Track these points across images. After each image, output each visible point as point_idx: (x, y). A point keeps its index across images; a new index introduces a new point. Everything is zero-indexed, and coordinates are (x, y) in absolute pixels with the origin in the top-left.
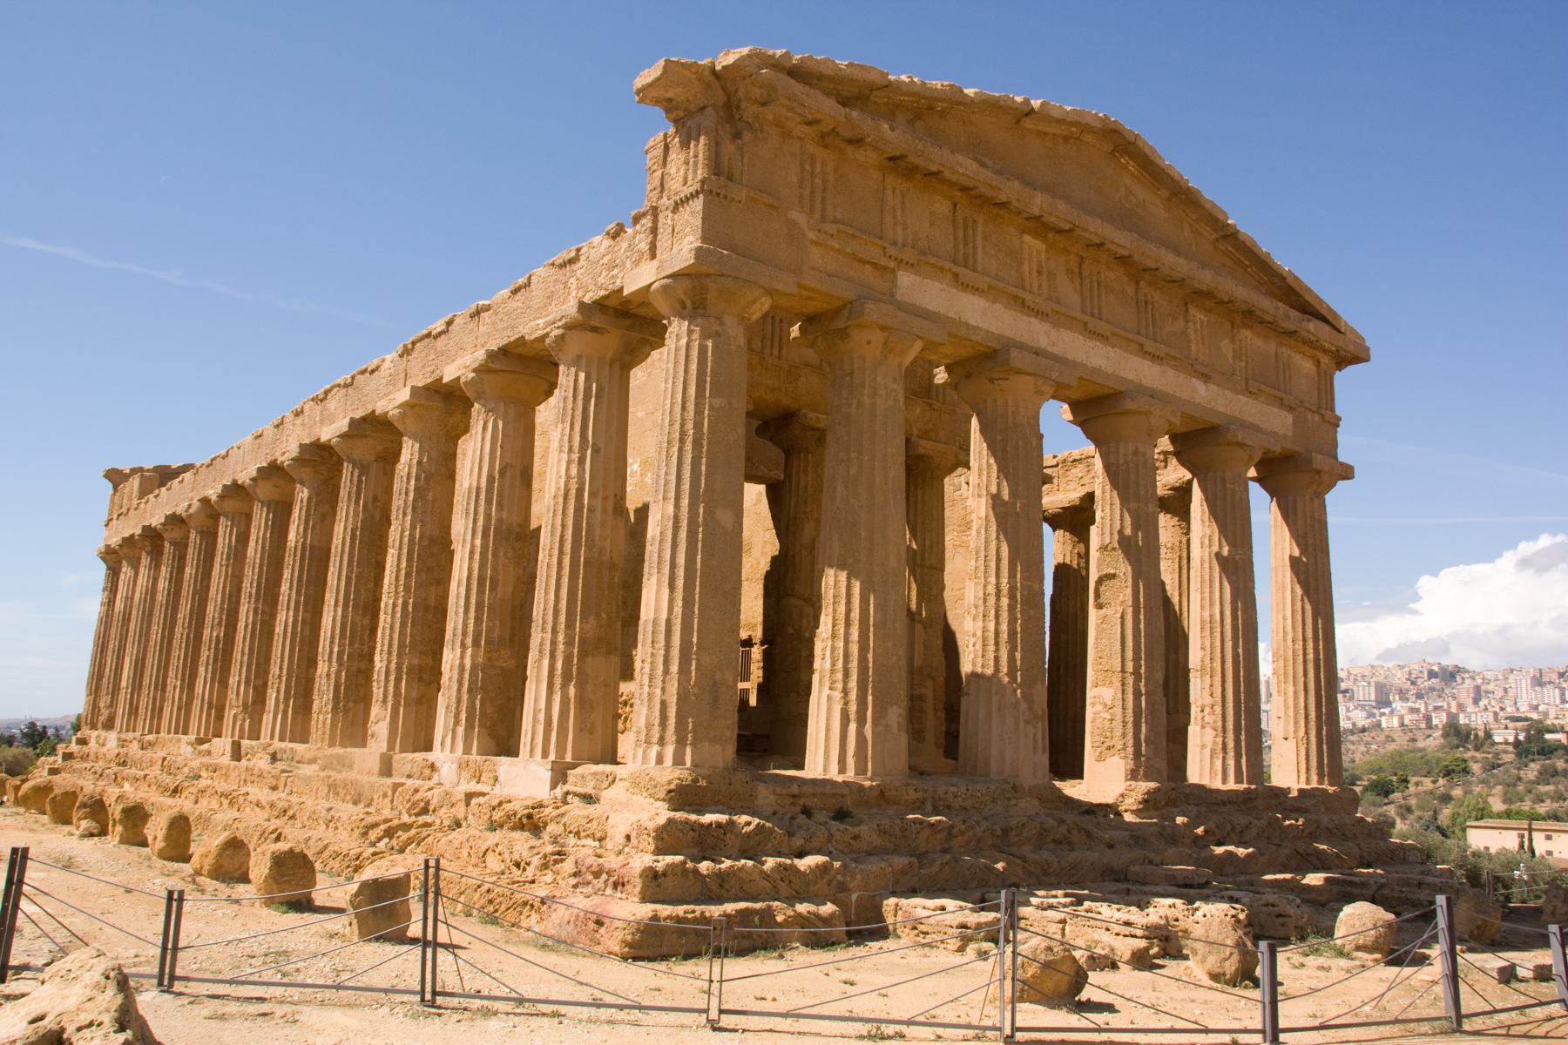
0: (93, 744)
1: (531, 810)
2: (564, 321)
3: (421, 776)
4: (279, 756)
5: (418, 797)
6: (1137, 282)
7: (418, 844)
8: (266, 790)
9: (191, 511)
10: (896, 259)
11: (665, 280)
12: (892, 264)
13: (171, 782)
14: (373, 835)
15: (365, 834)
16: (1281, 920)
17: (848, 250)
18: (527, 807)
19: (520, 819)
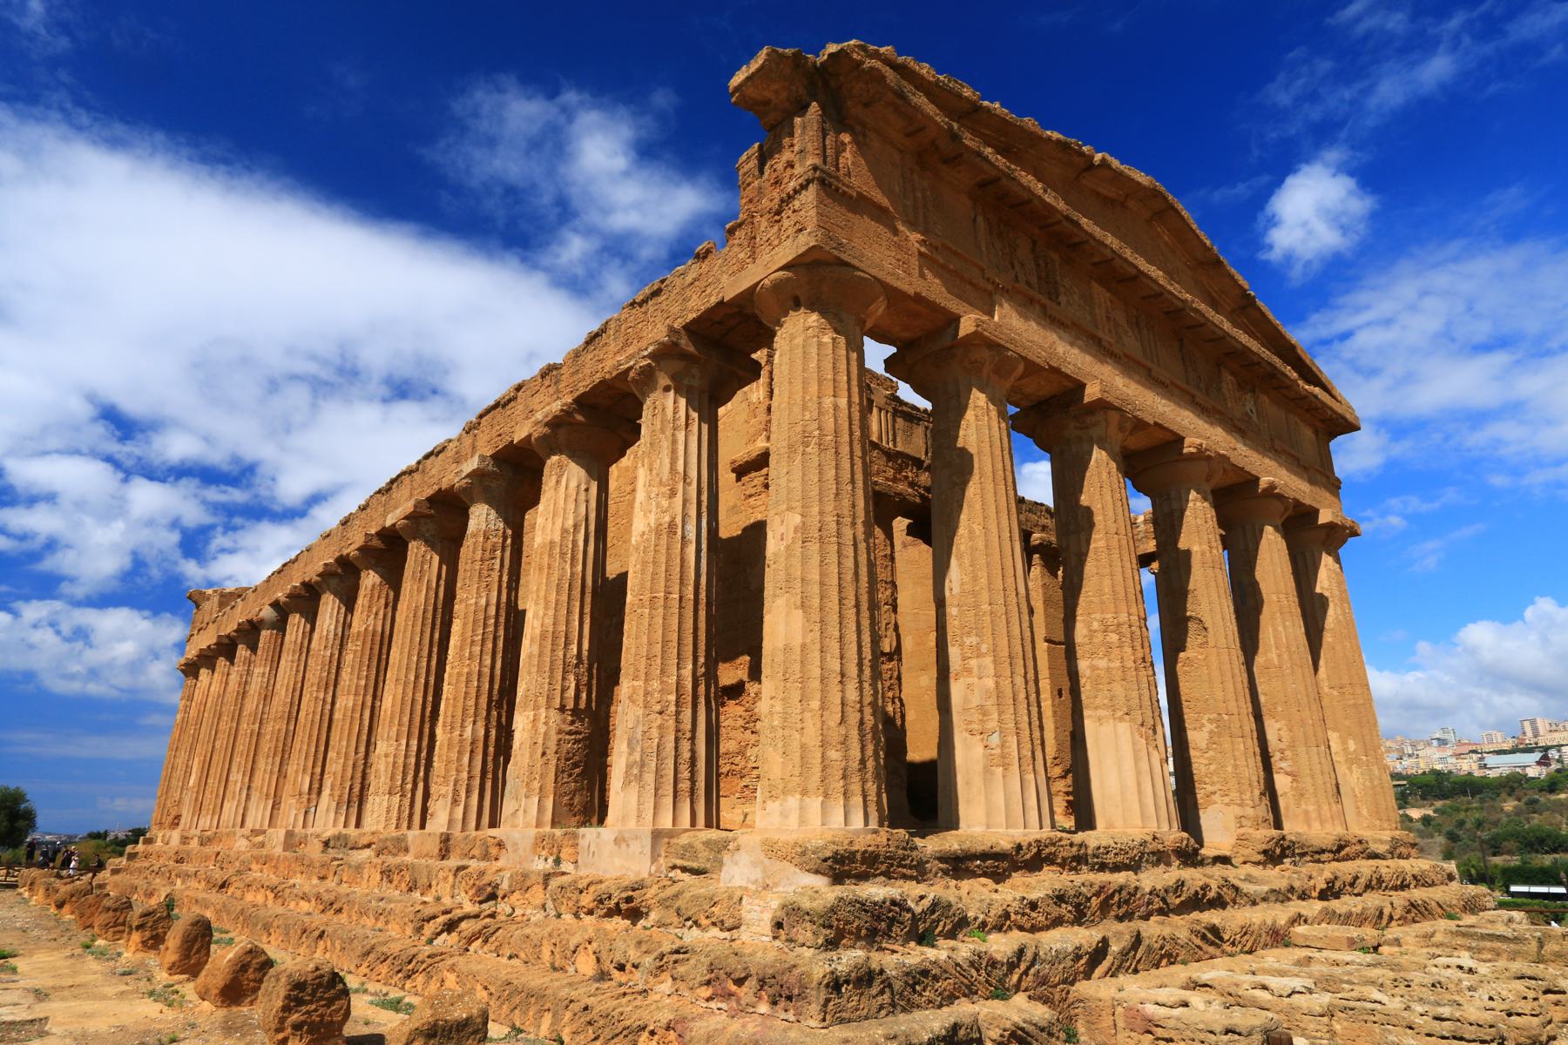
0: (159, 843)
1: (630, 893)
2: (651, 349)
3: (486, 856)
4: (331, 844)
5: (486, 880)
6: (1181, 340)
7: (486, 941)
8: (315, 881)
9: (262, 614)
10: (993, 283)
11: (781, 273)
12: (990, 287)
13: (219, 876)
14: (429, 929)
15: (419, 930)
16: (1551, 997)
17: (951, 267)
18: (626, 889)
19: (617, 904)
